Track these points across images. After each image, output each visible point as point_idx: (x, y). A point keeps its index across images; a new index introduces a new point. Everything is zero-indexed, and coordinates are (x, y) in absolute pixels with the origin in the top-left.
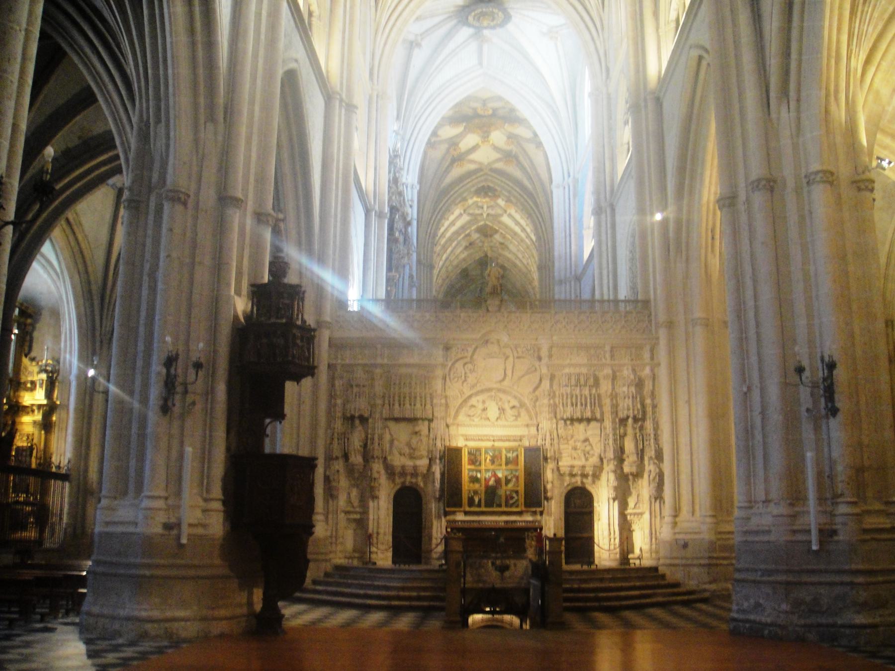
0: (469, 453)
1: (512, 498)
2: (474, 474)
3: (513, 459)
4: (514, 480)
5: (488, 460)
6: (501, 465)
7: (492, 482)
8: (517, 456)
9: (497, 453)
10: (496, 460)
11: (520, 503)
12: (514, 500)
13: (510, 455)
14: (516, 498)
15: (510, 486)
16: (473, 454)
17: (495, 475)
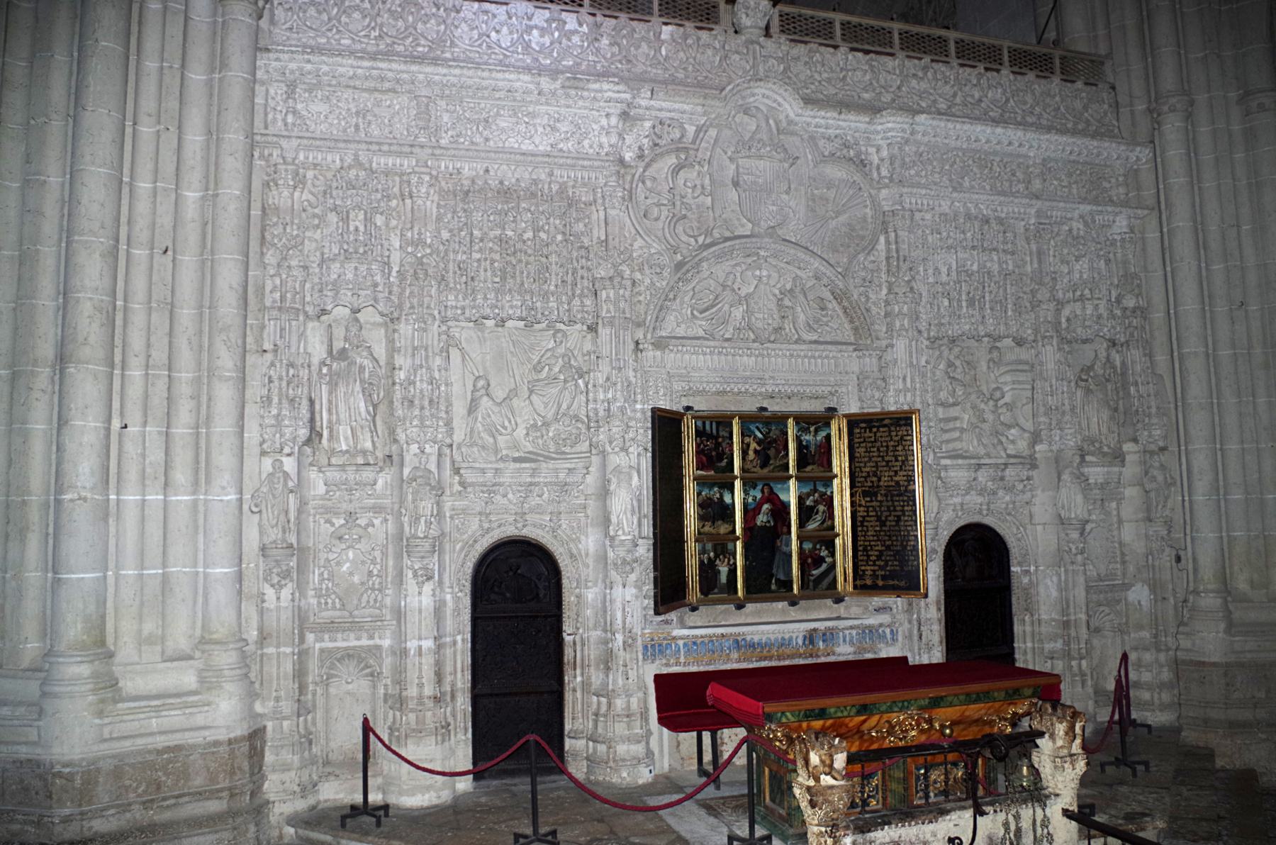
0: (700, 433)
1: (819, 561)
2: (715, 493)
3: (819, 446)
4: (821, 508)
5: (751, 453)
6: (786, 467)
7: (761, 519)
8: (828, 437)
9: (775, 433)
10: (772, 452)
11: (840, 579)
12: (824, 566)
13: (807, 438)
14: (829, 560)
15: (812, 526)
16: (709, 436)
17: (772, 498)
